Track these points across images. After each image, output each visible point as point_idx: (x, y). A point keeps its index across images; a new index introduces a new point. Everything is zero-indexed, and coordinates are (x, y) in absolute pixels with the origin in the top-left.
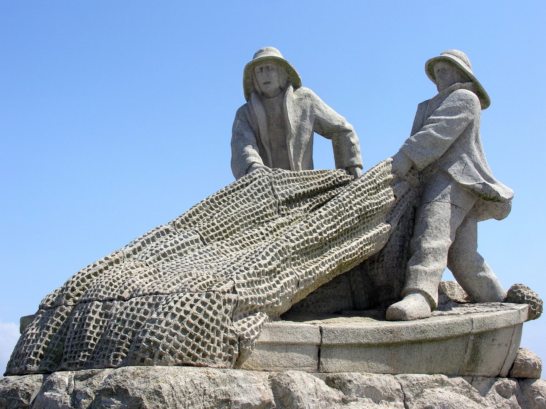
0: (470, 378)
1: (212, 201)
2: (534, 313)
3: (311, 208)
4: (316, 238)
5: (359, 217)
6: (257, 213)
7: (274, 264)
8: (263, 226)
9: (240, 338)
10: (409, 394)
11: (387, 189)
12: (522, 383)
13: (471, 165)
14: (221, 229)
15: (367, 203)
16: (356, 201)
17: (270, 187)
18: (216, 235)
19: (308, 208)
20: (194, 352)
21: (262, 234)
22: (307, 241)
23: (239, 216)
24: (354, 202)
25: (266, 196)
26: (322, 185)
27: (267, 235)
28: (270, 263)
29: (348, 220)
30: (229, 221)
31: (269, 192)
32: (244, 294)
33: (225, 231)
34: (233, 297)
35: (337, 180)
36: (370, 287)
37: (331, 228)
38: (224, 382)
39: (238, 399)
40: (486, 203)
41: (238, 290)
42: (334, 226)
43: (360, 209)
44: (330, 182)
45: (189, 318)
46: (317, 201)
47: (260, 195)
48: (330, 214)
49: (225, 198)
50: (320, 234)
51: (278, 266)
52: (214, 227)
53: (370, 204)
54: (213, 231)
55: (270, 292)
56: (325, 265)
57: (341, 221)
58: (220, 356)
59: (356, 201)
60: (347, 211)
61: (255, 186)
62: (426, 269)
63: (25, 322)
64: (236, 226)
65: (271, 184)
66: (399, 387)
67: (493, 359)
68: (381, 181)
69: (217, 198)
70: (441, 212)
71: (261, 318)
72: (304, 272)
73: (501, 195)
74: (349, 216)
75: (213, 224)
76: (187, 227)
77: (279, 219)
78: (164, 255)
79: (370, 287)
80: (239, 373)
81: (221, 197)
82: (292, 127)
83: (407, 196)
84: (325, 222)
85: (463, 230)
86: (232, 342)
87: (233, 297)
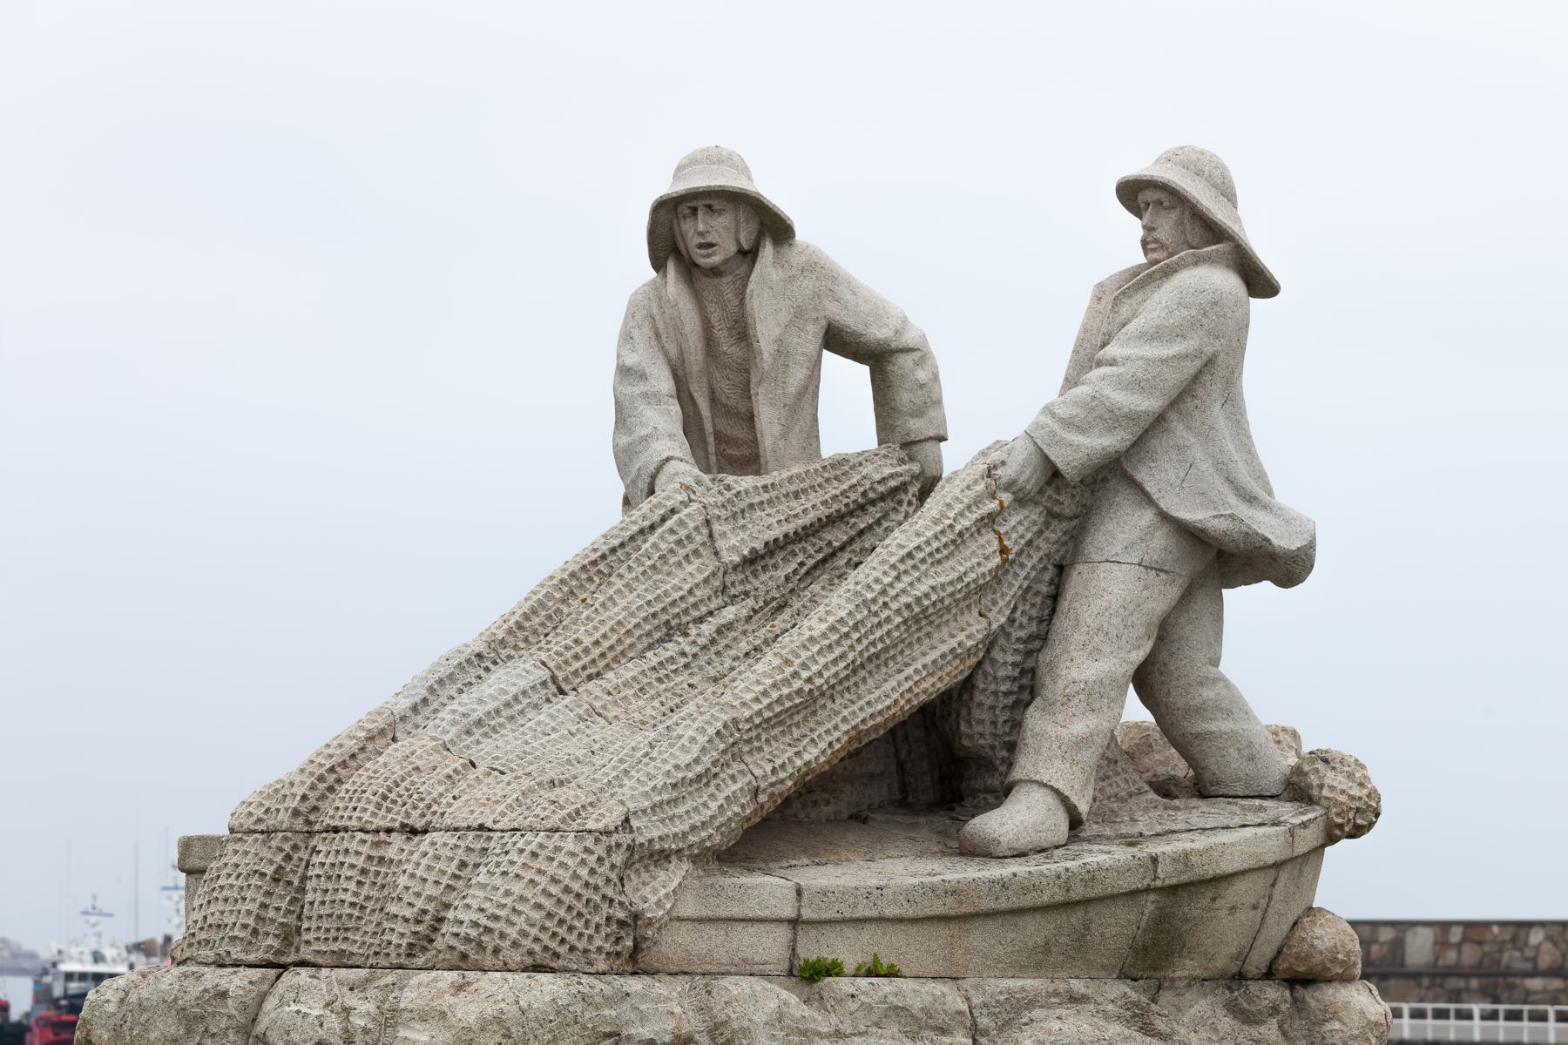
0: (1153, 983)
1: (573, 575)
2: (1356, 820)
3: (803, 571)
4: (799, 692)
5: (905, 622)
6: (673, 603)
7: (707, 759)
8: (686, 635)
9: (636, 916)
10: (984, 1021)
11: (981, 540)
12: (1300, 991)
13: (1205, 466)
14: (596, 652)
15: (923, 588)
16: (899, 586)
17: (705, 531)
18: (584, 668)
19: (795, 572)
20: (553, 945)
21: (684, 654)
22: (779, 701)
23: (632, 615)
24: (892, 592)
25: (696, 553)
26: (835, 507)
27: (695, 656)
28: (697, 761)
29: (878, 634)
30: (613, 630)
31: (704, 544)
32: (649, 831)
33: (603, 655)
34: (625, 839)
35: (872, 488)
36: (932, 766)
37: (835, 662)
38: (609, 1001)
39: (633, 1031)
40: (1231, 558)
41: (635, 823)
42: (843, 656)
43: (908, 606)
44: (853, 496)
45: (543, 881)
46: (820, 550)
47: (682, 552)
48: (833, 628)
49: (602, 567)
50: (809, 680)
51: (715, 763)
52: (578, 649)
53: (933, 588)
54: (576, 657)
55: (696, 819)
56: (815, 747)
57: (859, 640)
58: (599, 949)
59: (899, 586)
60: (876, 614)
61: (672, 531)
62: (1064, 733)
63: (195, 860)
64: (628, 641)
65: (708, 521)
66: (965, 1007)
67: (1225, 932)
68: (967, 523)
69: (584, 568)
70: (1118, 584)
71: (675, 874)
72: (769, 768)
73: (1275, 541)
74: (879, 625)
75: (577, 641)
76: (522, 645)
77: (725, 612)
78: (479, 723)
79: (932, 766)
80: (635, 985)
81: (594, 563)
82: (766, 356)
83: (1040, 542)
84: (820, 652)
85: (1182, 620)
86: (622, 924)
87: (625, 839)
